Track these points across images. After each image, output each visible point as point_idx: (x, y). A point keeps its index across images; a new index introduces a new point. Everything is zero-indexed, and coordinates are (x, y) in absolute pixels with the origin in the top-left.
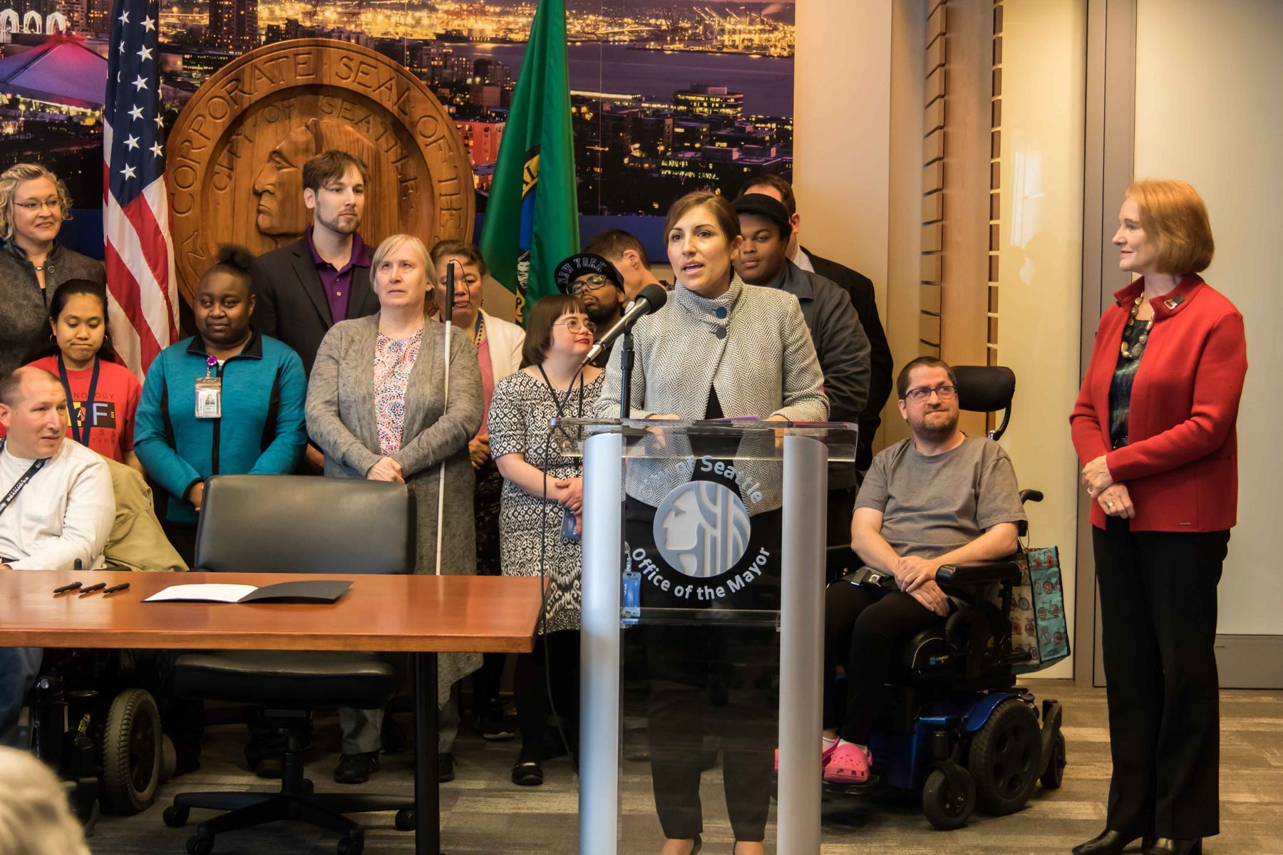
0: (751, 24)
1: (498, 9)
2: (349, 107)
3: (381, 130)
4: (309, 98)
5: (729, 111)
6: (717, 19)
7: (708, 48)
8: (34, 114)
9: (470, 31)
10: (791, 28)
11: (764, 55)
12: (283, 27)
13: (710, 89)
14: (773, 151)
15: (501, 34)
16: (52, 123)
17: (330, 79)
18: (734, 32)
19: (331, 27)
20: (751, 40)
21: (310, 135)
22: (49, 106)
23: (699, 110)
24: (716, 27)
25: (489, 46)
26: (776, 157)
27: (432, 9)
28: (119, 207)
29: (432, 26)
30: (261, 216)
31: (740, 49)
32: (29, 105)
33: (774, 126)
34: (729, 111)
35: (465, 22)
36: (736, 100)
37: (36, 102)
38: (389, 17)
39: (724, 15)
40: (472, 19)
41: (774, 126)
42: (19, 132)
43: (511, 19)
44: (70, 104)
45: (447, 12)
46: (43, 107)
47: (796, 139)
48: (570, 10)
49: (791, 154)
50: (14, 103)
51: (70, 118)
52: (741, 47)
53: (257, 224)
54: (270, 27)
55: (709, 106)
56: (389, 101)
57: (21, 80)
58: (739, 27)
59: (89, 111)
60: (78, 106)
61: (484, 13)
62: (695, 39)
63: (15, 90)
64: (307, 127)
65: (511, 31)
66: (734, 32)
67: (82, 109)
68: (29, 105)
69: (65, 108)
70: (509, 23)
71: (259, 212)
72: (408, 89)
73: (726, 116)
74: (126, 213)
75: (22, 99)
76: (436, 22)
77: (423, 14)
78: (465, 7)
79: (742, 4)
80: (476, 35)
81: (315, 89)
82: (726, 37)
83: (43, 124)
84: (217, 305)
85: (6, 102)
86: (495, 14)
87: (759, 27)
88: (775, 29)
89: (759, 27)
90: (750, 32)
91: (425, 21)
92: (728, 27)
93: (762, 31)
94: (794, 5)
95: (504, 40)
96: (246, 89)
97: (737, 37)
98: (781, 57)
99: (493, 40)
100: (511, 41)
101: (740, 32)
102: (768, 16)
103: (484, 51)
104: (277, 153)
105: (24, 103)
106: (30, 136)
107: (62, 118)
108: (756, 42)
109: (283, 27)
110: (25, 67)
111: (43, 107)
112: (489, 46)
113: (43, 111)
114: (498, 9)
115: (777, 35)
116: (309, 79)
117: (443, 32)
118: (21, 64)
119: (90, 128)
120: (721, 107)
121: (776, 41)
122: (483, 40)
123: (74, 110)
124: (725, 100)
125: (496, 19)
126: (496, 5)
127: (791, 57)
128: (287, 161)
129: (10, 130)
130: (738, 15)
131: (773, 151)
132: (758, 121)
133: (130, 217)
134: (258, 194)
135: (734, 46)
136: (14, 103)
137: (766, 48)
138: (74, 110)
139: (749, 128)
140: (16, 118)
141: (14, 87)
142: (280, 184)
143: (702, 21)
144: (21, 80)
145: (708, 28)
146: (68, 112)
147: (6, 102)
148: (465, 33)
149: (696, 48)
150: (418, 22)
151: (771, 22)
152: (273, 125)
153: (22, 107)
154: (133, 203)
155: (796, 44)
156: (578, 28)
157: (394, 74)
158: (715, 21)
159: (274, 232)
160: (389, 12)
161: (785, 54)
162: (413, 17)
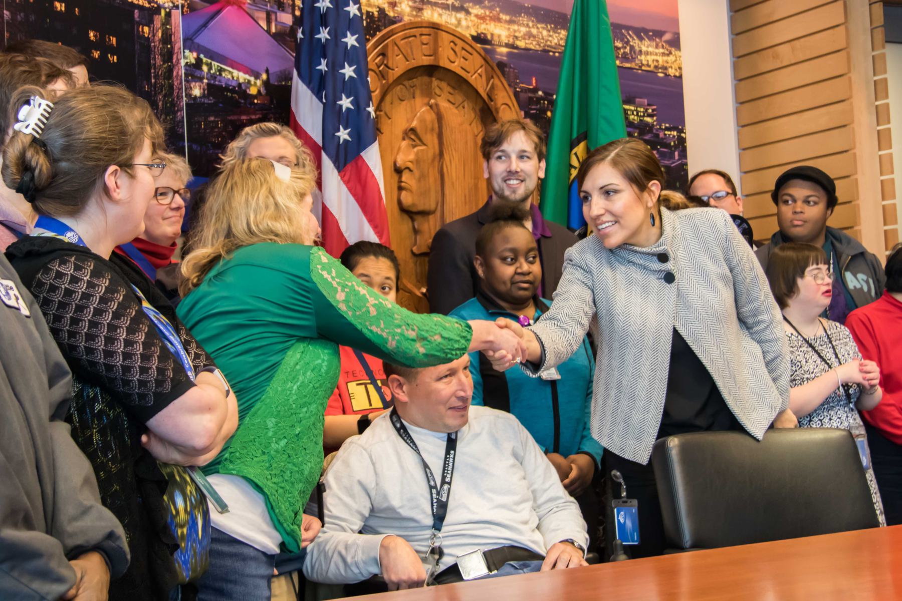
0: (657, 47)
1: (508, 18)
2: (452, 91)
3: (473, 115)
4: (426, 79)
5: (649, 120)
6: (637, 41)
7: (632, 65)
8: (214, 77)
9: (492, 35)
10: (677, 53)
11: (666, 74)
12: (376, 14)
13: (637, 100)
14: (676, 153)
15: (511, 41)
16: (227, 89)
17: (444, 63)
18: (647, 53)
19: (406, 19)
20: (657, 61)
21: (434, 116)
22: (225, 70)
23: (632, 117)
24: (637, 49)
25: (504, 50)
26: (679, 160)
27: (468, 12)
28: (336, 171)
29: (468, 27)
30: (404, 193)
31: (652, 68)
32: (210, 67)
33: (675, 133)
34: (649, 120)
35: (488, 27)
36: (653, 110)
37: (215, 64)
38: (440, 15)
39: (641, 39)
40: (493, 24)
41: (675, 133)
42: (203, 96)
43: (516, 27)
44: (239, 70)
45: (477, 16)
46: (221, 70)
47: (689, 144)
48: (550, 24)
49: (685, 157)
50: (199, 63)
51: (240, 85)
52: (652, 66)
53: (399, 202)
54: (368, 12)
55: (637, 115)
56: (481, 87)
57: (201, 40)
58: (650, 49)
59: (252, 79)
60: (245, 73)
61: (499, 20)
62: (625, 58)
63: (199, 49)
64: (431, 107)
65: (517, 38)
66: (647, 53)
67: (247, 77)
68: (210, 68)
69: (236, 73)
70: (515, 31)
71: (400, 189)
72: (492, 77)
73: (647, 124)
74: (342, 178)
75: (205, 60)
76: (470, 24)
77: (461, 15)
78: (488, 13)
79: (650, 31)
80: (496, 40)
81: (432, 70)
82: (643, 57)
83: (220, 88)
84: (522, 260)
85: (193, 61)
86: (506, 21)
87: (661, 50)
88: (670, 53)
89: (661, 50)
90: (656, 54)
91: (464, 23)
92: (644, 49)
93: (663, 54)
94: (678, 34)
95: (512, 46)
96: (390, 65)
97: (650, 58)
98: (675, 76)
99: (507, 45)
100: (517, 48)
101: (651, 54)
102: (666, 42)
103: (501, 54)
104: (413, 130)
105: (207, 64)
106: (211, 100)
107: (234, 84)
108: (661, 63)
109: (376, 14)
110: (205, 25)
111: (221, 70)
112: (504, 50)
113: (220, 75)
114: (508, 18)
115: (671, 58)
116: (426, 61)
117: (475, 34)
118: (201, 21)
119: (255, 97)
120: (644, 116)
121: (671, 62)
122: (501, 46)
123: (242, 77)
124: (646, 110)
125: (507, 26)
126: (507, 14)
127: (681, 77)
128: (420, 140)
129: (197, 92)
130: (649, 39)
131: (676, 153)
132: (667, 129)
133: (347, 183)
134: (398, 171)
135: (648, 66)
136: (199, 63)
137: (666, 68)
138: (242, 77)
139: (661, 135)
140: (201, 79)
141: (199, 45)
142: (417, 161)
143: (628, 43)
144: (201, 40)
145: (632, 48)
146: (238, 78)
147: (193, 61)
148: (489, 37)
149: (627, 65)
150: (459, 21)
151: (667, 47)
152: (404, 103)
153: (205, 68)
154: (349, 167)
155: (683, 67)
156: (556, 41)
157: (483, 62)
158: (635, 42)
159: (414, 210)
160: (439, 10)
161: (677, 74)
162: (456, 18)
